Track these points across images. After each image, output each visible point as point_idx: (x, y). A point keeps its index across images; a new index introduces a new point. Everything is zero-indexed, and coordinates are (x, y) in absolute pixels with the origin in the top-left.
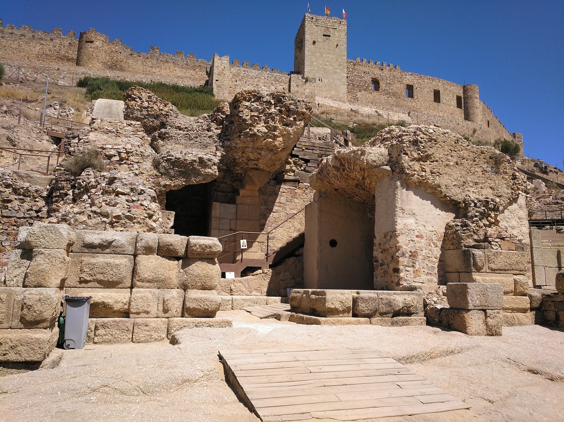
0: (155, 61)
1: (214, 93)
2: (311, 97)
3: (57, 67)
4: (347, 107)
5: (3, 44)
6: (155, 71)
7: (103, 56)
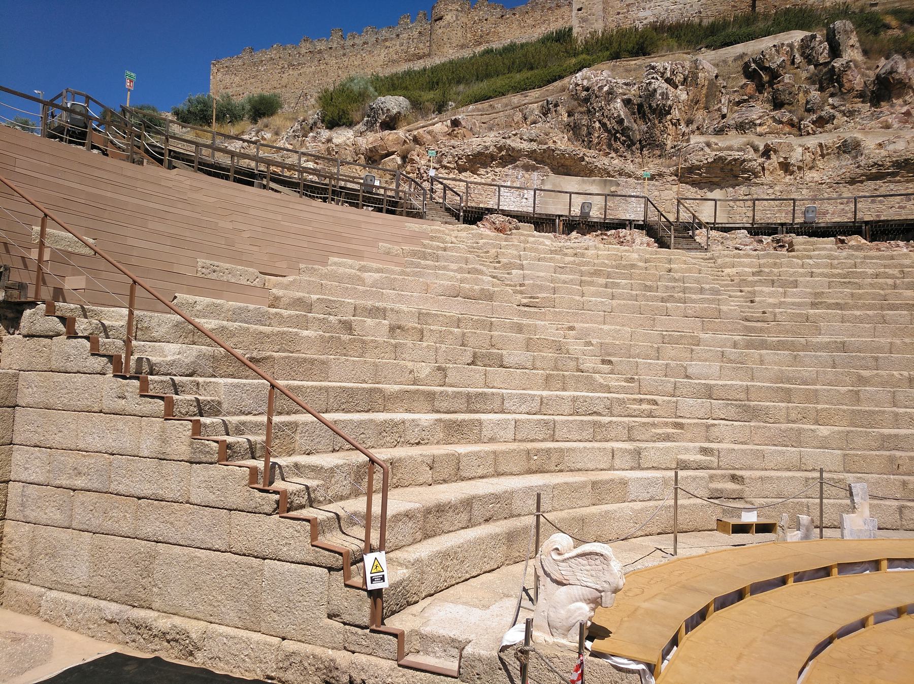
0: (538, 15)
5: (346, 64)
7: (460, 34)
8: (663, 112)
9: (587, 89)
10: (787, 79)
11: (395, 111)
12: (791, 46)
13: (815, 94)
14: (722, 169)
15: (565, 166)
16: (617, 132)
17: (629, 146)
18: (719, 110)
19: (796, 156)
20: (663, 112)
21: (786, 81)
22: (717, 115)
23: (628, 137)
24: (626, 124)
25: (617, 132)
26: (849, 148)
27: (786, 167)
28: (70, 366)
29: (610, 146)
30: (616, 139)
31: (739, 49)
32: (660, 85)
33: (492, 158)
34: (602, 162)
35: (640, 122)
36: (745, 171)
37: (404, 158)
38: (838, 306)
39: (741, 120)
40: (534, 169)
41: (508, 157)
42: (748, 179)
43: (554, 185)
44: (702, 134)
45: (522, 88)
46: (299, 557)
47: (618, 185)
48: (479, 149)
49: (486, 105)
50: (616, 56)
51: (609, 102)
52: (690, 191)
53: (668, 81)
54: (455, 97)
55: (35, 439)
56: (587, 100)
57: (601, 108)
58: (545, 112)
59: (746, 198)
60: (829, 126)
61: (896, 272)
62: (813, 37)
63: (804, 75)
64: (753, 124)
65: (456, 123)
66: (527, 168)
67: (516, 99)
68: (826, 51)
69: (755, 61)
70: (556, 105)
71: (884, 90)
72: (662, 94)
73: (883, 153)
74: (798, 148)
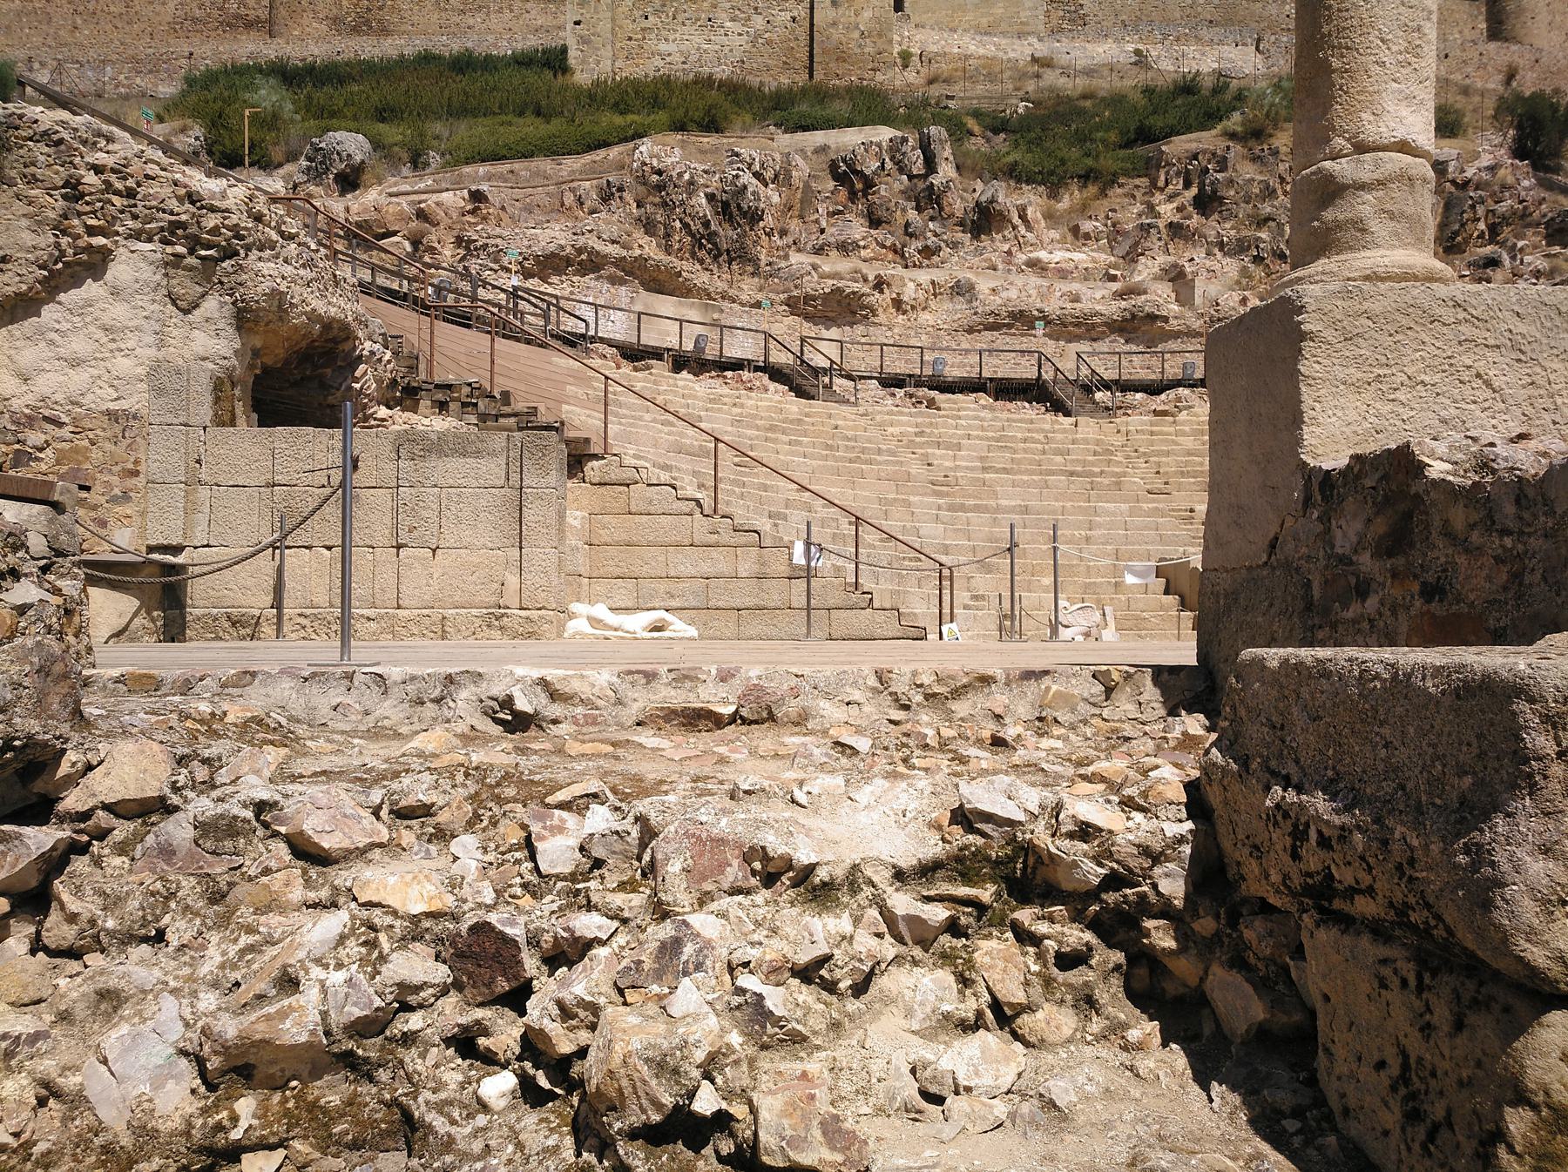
1: (572, 62)
2: (880, 35)
3: (187, 50)
4: (1021, 51)
6: (471, 21)
8: (754, 217)
9: (659, 173)
10: (883, 190)
11: (358, 158)
12: (879, 145)
13: (912, 214)
14: (839, 302)
15: (660, 282)
16: (703, 237)
17: (716, 258)
18: (817, 221)
19: (909, 292)
20: (754, 217)
21: (883, 193)
22: (814, 228)
23: (715, 244)
24: (713, 227)
25: (703, 237)
26: (962, 290)
27: (898, 304)
28: (652, 509)
29: (693, 255)
30: (701, 246)
31: (818, 137)
32: (747, 178)
33: (568, 262)
34: (702, 278)
35: (726, 225)
36: (863, 307)
37: (416, 243)
38: (1005, 471)
39: (842, 238)
40: (622, 282)
41: (591, 264)
42: (866, 317)
43: (645, 305)
44: (799, 250)
45: (555, 150)
46: (890, 634)
47: (722, 311)
48: (552, 248)
49: (504, 167)
50: (680, 127)
51: (690, 195)
52: (808, 329)
53: (757, 175)
54: (435, 143)
55: (618, 572)
56: (660, 187)
57: (682, 203)
58: (606, 198)
59: (863, 340)
60: (935, 259)
61: (1041, 437)
62: (905, 140)
63: (897, 186)
64: (857, 246)
65: (477, 197)
66: (613, 280)
67: (545, 164)
68: (921, 161)
69: (844, 160)
70: (621, 189)
71: (984, 221)
72: (754, 193)
73: (999, 301)
74: (912, 282)
